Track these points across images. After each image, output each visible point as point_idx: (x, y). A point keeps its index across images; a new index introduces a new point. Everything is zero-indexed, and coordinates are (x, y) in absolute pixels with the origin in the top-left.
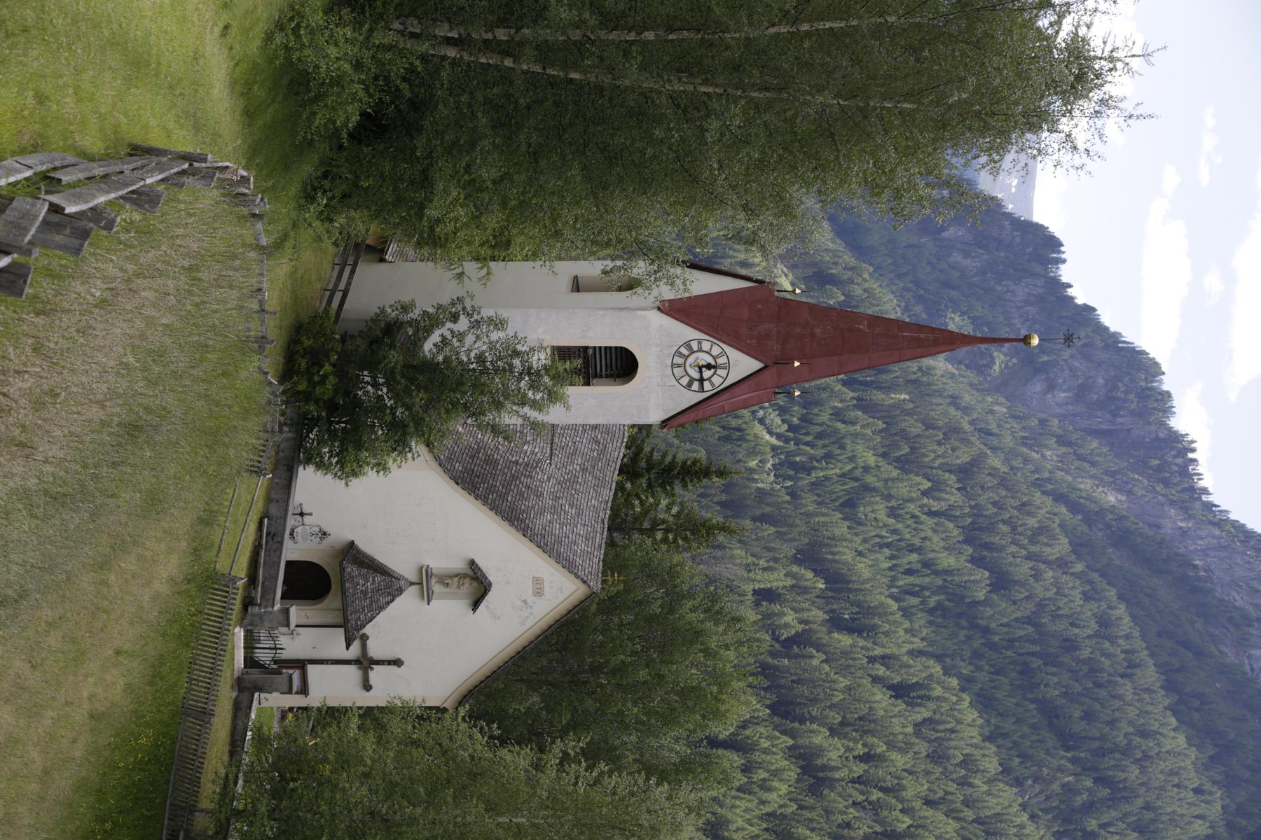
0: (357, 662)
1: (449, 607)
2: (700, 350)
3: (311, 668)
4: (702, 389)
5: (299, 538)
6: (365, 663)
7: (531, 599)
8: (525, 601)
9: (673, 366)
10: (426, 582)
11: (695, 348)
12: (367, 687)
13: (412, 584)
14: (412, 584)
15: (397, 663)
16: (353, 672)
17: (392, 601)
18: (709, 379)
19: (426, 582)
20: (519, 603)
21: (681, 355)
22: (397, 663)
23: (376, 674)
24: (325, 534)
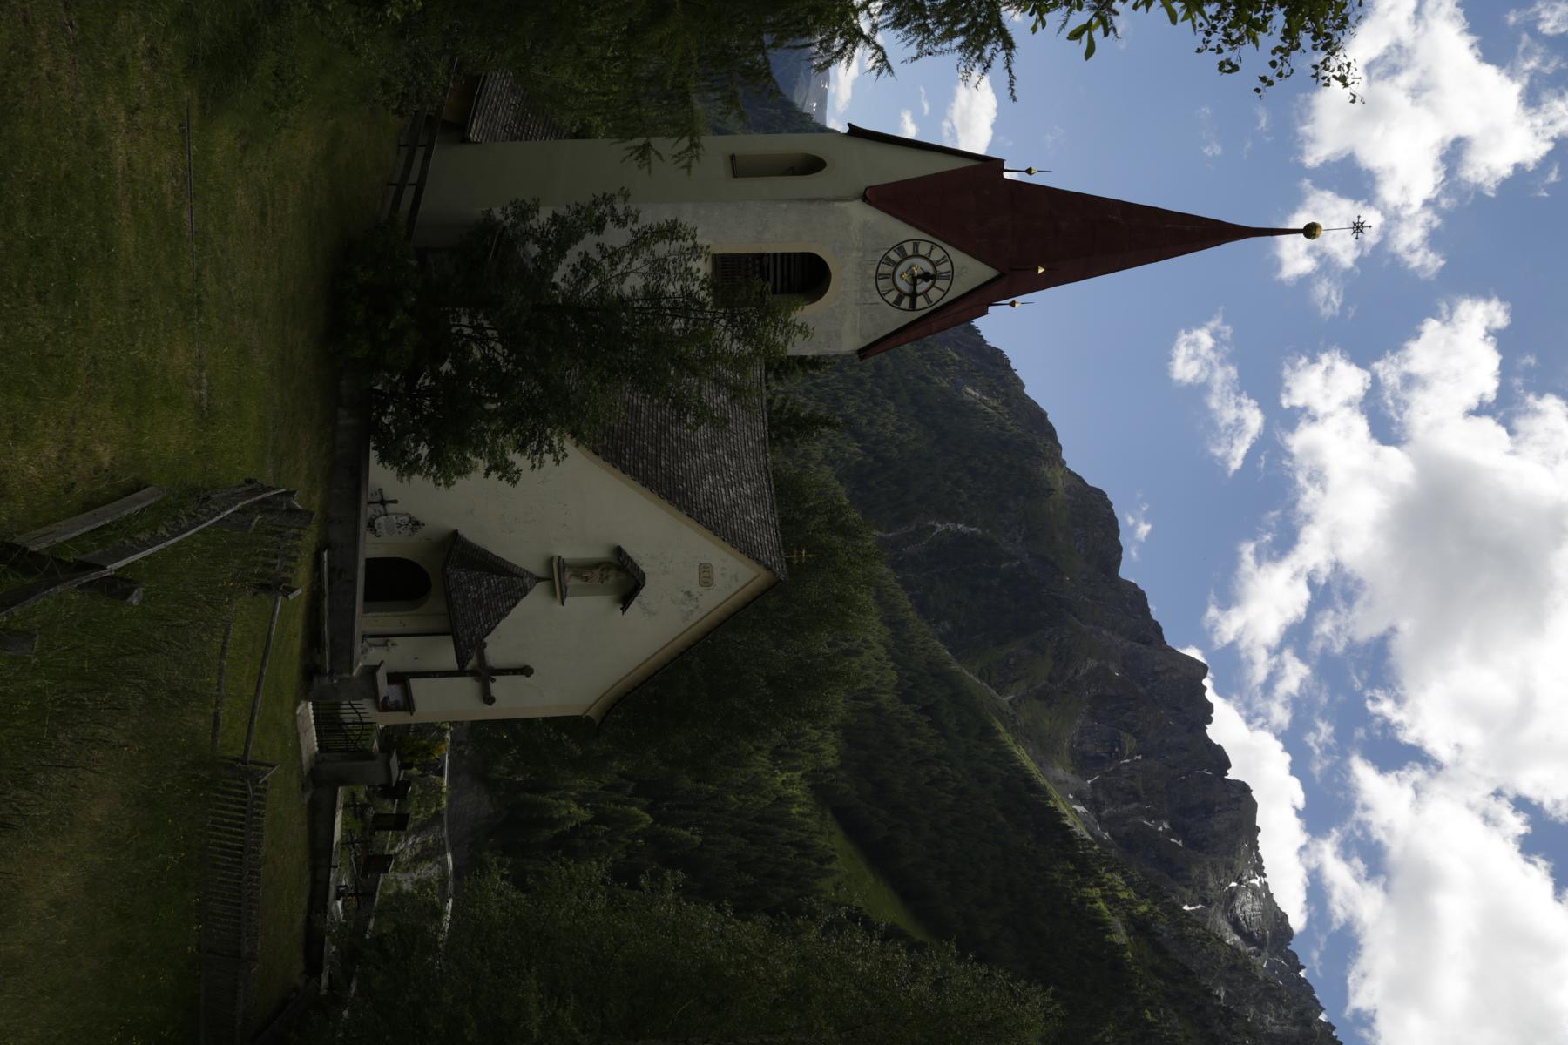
0: (472, 673)
1: (590, 607)
2: (916, 255)
3: (413, 682)
4: (913, 307)
5: (383, 530)
6: (485, 674)
7: (696, 589)
8: (688, 593)
9: (878, 276)
10: (559, 576)
11: (909, 252)
12: (488, 699)
13: (539, 579)
14: (539, 579)
15: (526, 671)
16: (467, 685)
17: (515, 605)
18: (925, 293)
19: (559, 576)
20: (681, 595)
21: (886, 260)
22: (526, 671)
23: (499, 686)
24: (417, 523)
